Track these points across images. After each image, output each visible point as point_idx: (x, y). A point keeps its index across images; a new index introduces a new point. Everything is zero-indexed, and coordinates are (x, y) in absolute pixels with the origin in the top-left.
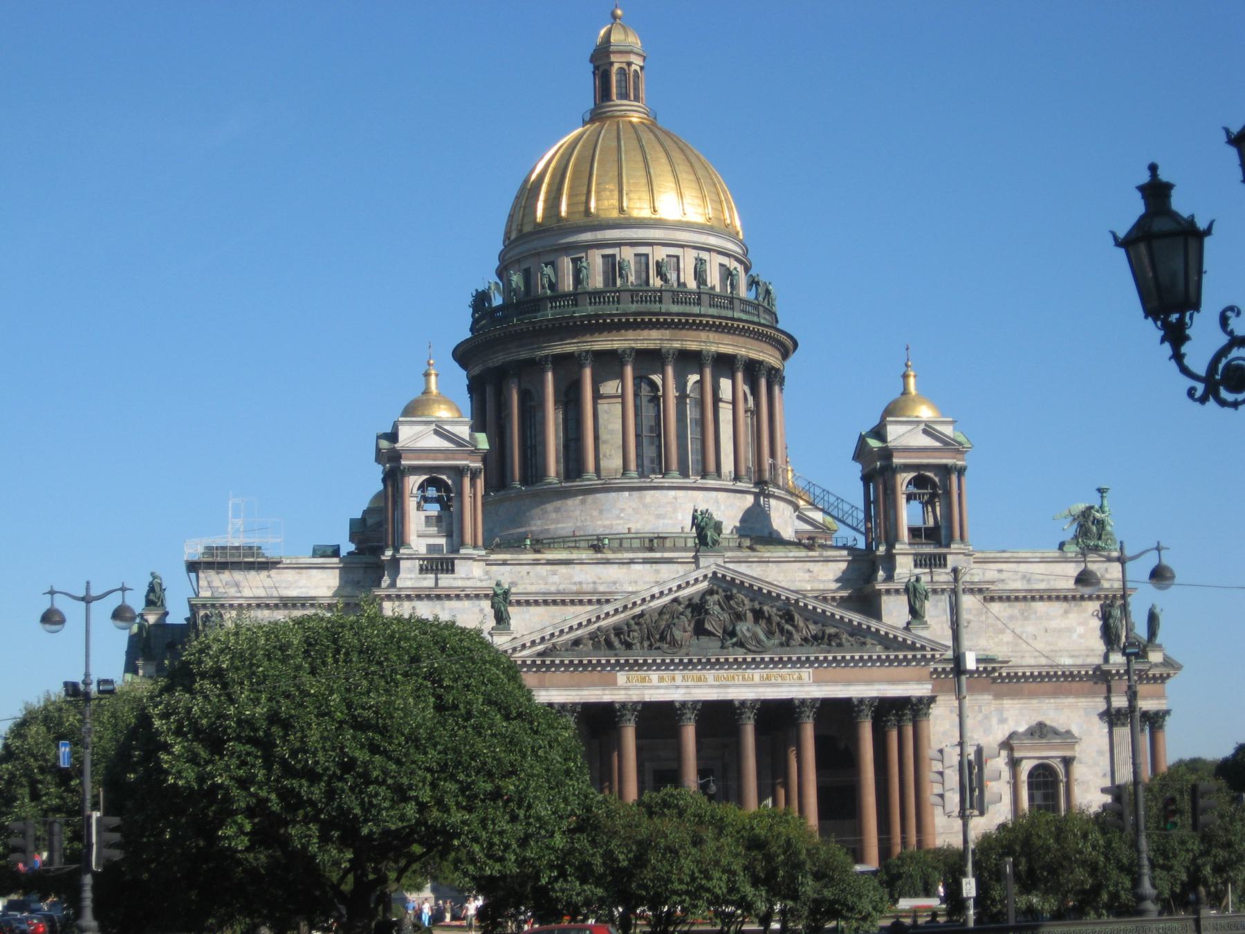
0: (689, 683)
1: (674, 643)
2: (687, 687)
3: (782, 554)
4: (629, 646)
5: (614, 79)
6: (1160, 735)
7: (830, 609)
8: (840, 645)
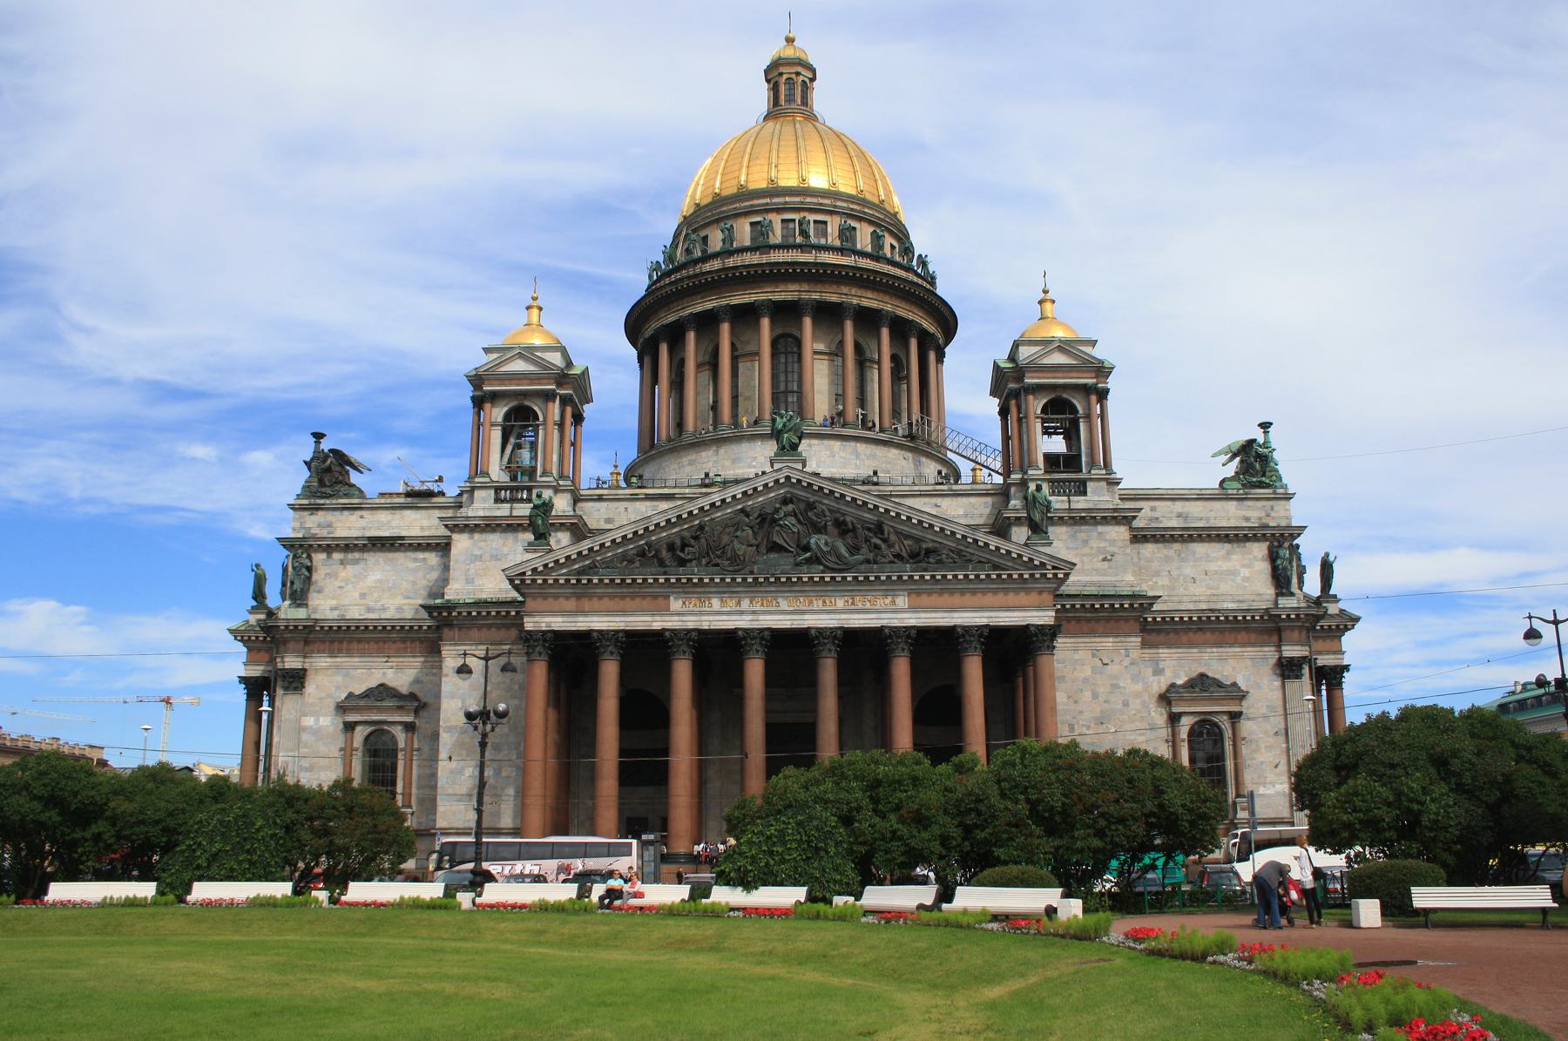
0: (758, 608)
1: (734, 559)
2: (754, 612)
4: (683, 562)
5: (782, 88)
6: (1337, 692)
7: (925, 518)
8: (939, 562)
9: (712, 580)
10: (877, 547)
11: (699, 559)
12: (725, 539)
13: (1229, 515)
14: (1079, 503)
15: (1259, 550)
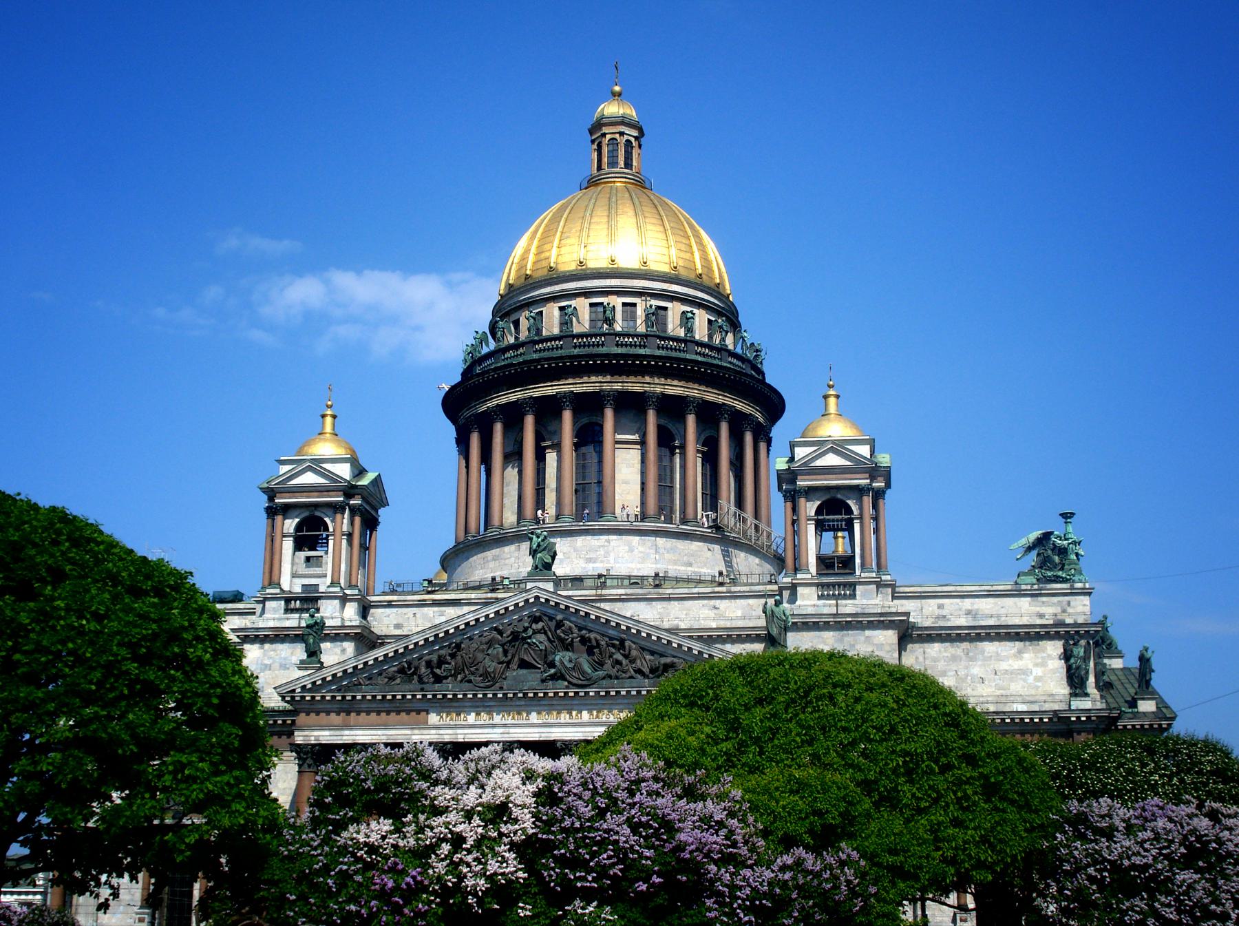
0: (510, 721)
1: (485, 675)
2: (505, 726)
3: (686, 591)
4: (438, 679)
5: (605, 150)
7: (664, 635)
9: (465, 695)
10: (618, 662)
11: (455, 676)
12: (480, 656)
13: (1022, 611)
14: (848, 607)
15: (1054, 648)
